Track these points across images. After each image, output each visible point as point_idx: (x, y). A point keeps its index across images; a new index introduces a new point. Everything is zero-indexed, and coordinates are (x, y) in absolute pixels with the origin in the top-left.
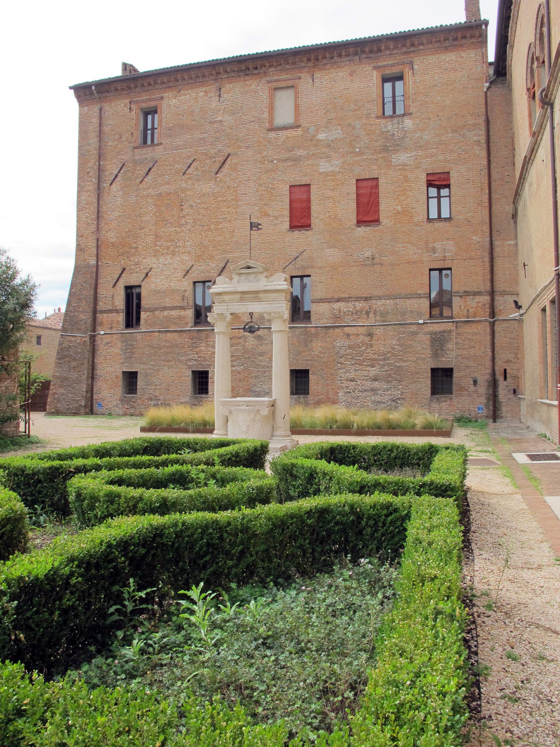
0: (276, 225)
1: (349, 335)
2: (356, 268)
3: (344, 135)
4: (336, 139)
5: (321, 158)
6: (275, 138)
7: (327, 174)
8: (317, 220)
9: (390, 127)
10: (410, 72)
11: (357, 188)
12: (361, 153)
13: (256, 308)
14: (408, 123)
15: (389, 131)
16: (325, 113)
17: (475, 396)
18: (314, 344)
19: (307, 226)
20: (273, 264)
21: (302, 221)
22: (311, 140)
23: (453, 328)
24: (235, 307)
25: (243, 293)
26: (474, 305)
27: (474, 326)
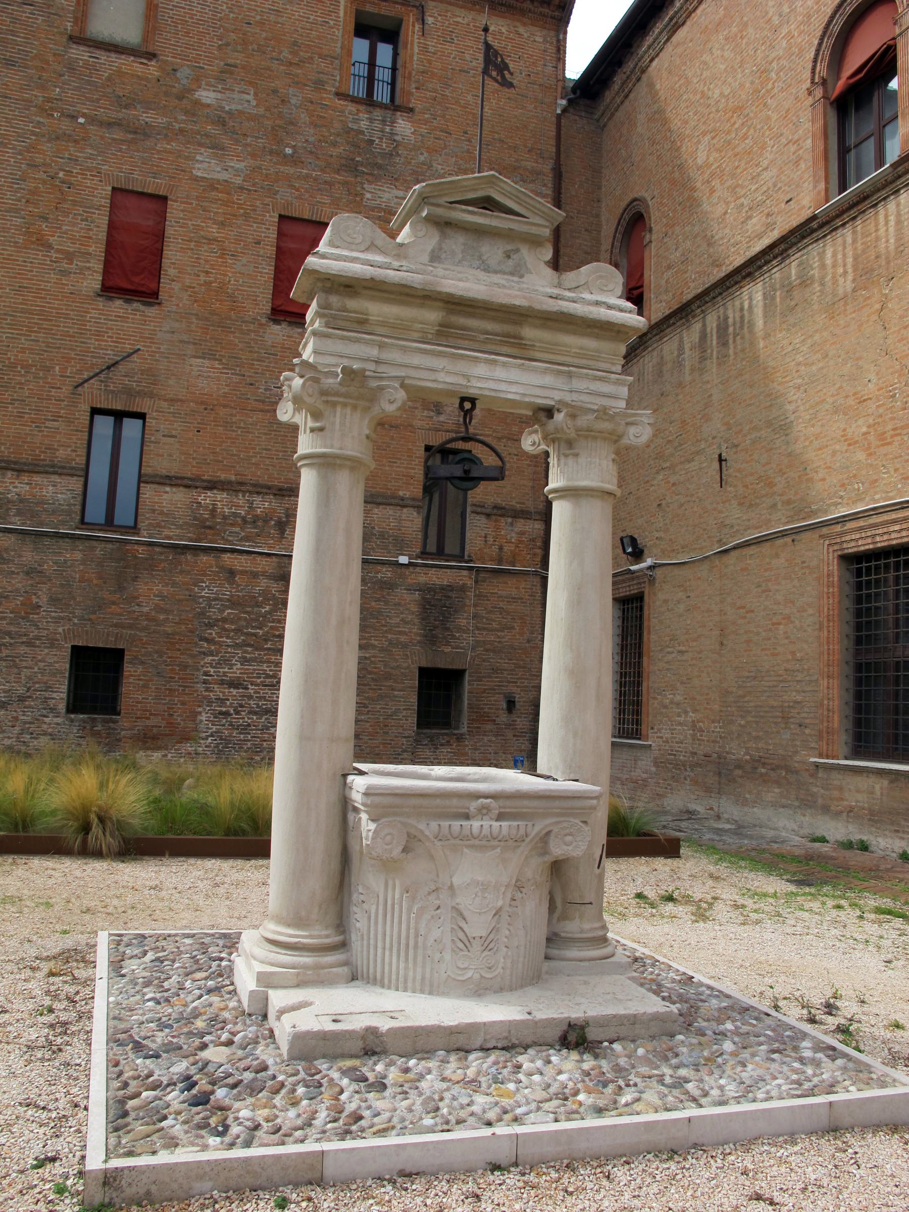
0: (65, 273)
1: (232, 573)
2: (260, 415)
3: (261, 111)
4: (240, 112)
5: (201, 145)
6: (86, 63)
7: (212, 185)
8: (176, 286)
9: (364, 124)
10: (417, 27)
11: (281, 234)
12: (295, 160)
13: (504, 381)
14: (403, 127)
15: (362, 133)
16: (220, 48)
17: (509, 734)
18: (142, 588)
19: (149, 295)
20: (48, 369)
21: (136, 279)
22: (180, 97)
23: (470, 583)
24: (417, 360)
25: (456, 305)
26: (514, 537)
27: (512, 581)
